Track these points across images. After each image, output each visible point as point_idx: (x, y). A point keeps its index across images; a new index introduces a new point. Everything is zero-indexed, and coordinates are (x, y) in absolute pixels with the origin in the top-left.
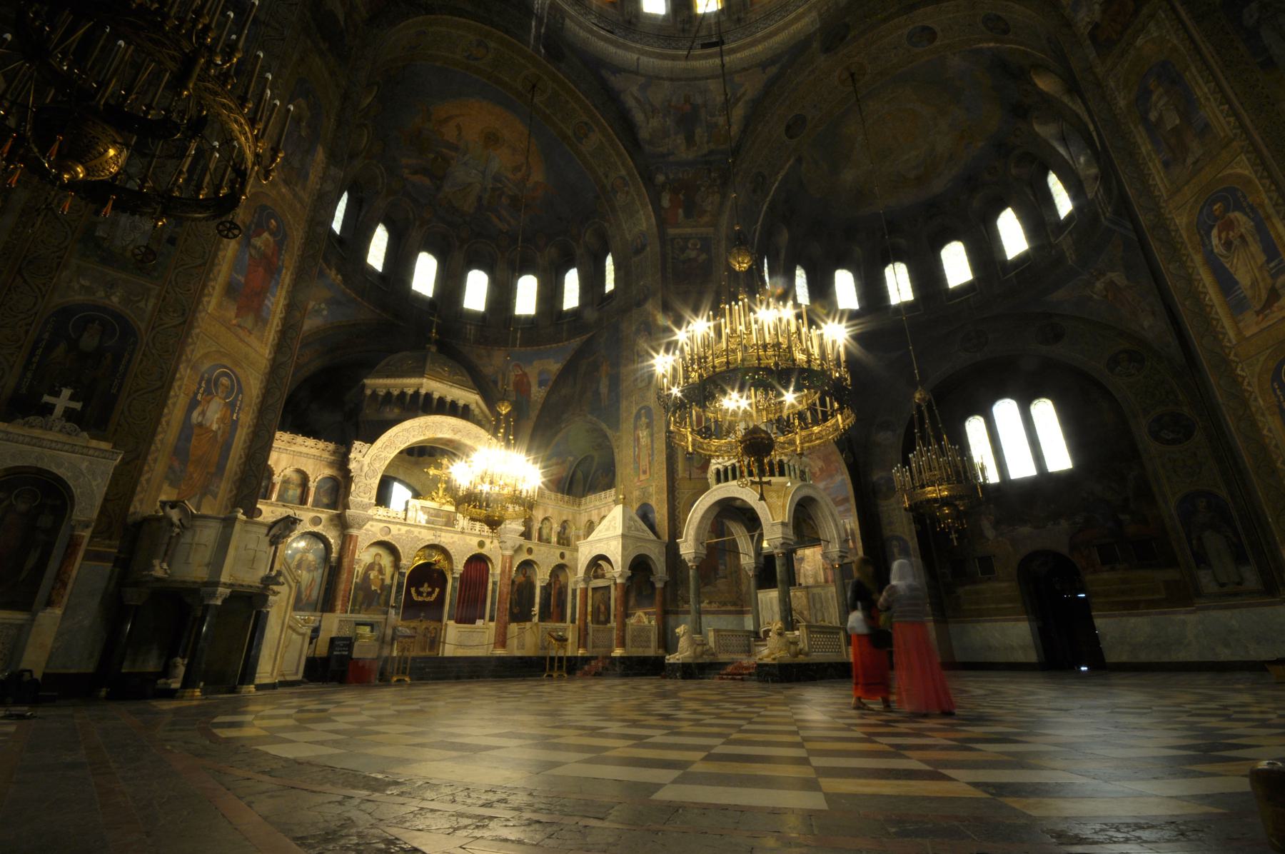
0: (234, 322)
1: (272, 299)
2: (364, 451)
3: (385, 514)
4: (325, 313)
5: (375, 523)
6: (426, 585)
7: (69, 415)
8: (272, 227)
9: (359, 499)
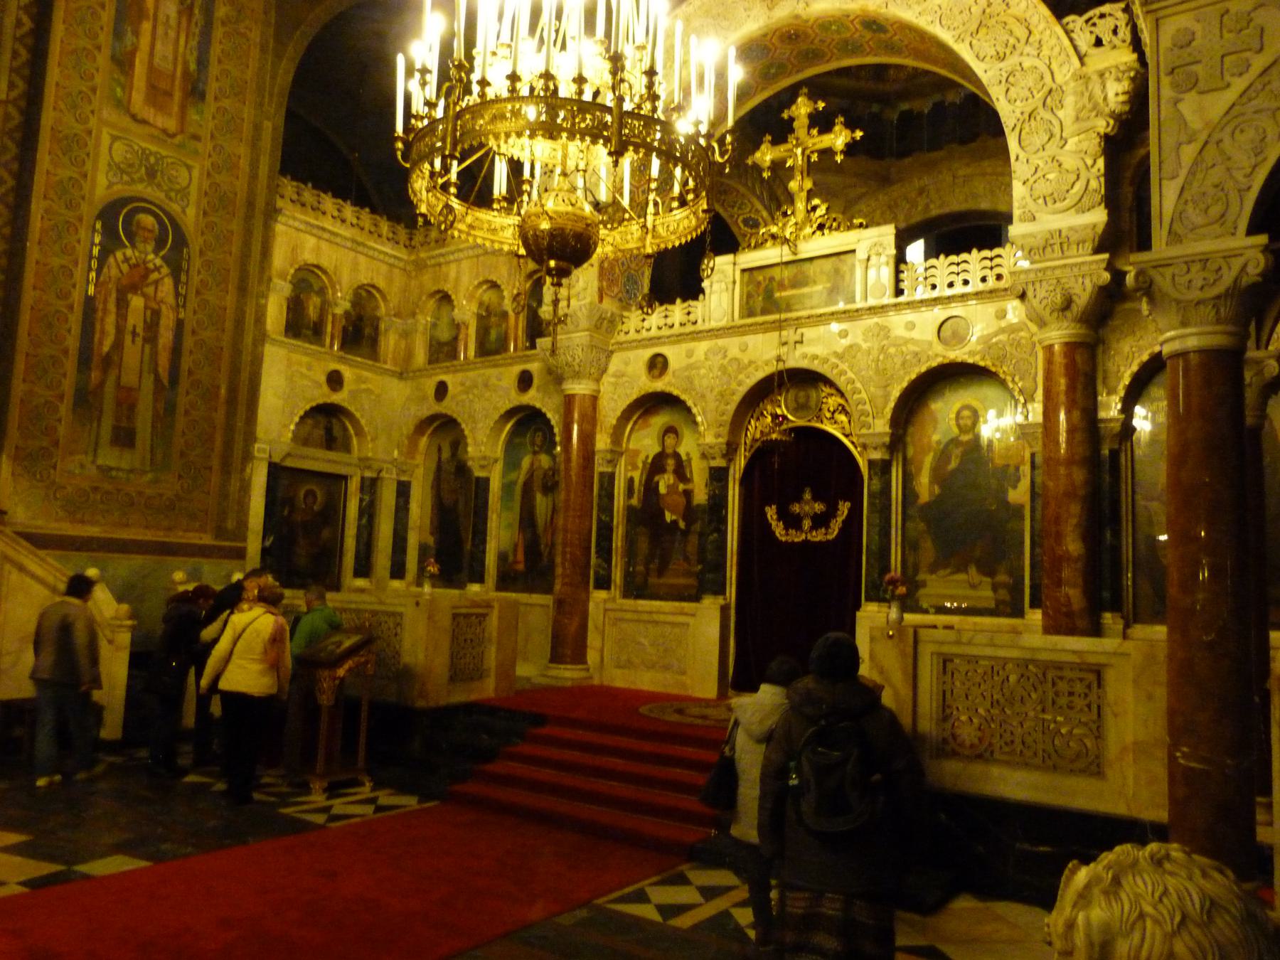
5: (631, 355)
6: (807, 496)
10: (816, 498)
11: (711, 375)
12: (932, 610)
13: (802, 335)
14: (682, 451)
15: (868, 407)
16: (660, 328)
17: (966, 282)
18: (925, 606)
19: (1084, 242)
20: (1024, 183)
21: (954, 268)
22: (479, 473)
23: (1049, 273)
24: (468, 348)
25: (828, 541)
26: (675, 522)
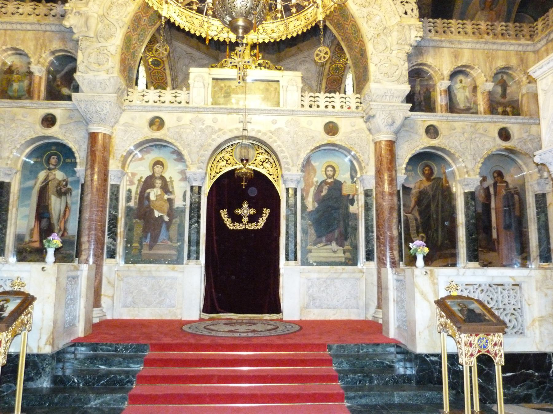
3: (157, 99)
5: (137, 114)
6: (245, 205)
10: (250, 207)
11: (194, 133)
12: (315, 264)
13: (251, 119)
14: (167, 176)
15: (289, 160)
16: (155, 102)
17: (333, 107)
18: (311, 262)
19: (399, 97)
20: (376, 65)
21: (328, 99)
23: (387, 108)
25: (258, 229)
26: (161, 217)
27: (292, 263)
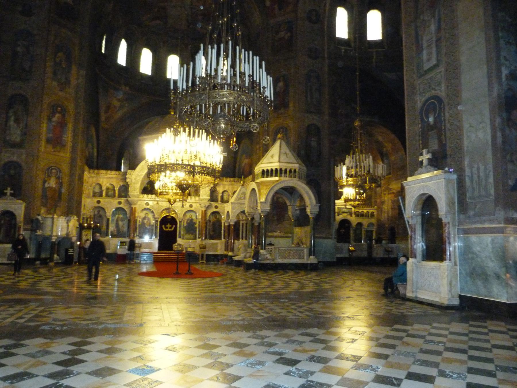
0: (52, 151)
1: (66, 136)
2: (132, 173)
4: (127, 105)
6: (169, 224)
7: (11, 195)
8: (58, 111)
9: (133, 193)
22: (108, 218)
24: (104, 194)
27: (180, 239)
